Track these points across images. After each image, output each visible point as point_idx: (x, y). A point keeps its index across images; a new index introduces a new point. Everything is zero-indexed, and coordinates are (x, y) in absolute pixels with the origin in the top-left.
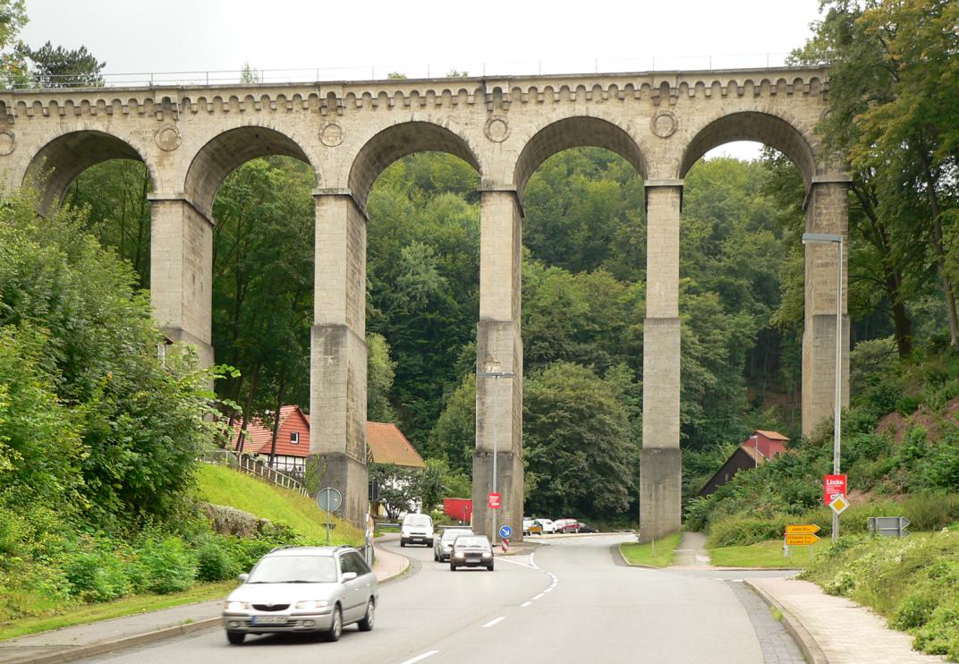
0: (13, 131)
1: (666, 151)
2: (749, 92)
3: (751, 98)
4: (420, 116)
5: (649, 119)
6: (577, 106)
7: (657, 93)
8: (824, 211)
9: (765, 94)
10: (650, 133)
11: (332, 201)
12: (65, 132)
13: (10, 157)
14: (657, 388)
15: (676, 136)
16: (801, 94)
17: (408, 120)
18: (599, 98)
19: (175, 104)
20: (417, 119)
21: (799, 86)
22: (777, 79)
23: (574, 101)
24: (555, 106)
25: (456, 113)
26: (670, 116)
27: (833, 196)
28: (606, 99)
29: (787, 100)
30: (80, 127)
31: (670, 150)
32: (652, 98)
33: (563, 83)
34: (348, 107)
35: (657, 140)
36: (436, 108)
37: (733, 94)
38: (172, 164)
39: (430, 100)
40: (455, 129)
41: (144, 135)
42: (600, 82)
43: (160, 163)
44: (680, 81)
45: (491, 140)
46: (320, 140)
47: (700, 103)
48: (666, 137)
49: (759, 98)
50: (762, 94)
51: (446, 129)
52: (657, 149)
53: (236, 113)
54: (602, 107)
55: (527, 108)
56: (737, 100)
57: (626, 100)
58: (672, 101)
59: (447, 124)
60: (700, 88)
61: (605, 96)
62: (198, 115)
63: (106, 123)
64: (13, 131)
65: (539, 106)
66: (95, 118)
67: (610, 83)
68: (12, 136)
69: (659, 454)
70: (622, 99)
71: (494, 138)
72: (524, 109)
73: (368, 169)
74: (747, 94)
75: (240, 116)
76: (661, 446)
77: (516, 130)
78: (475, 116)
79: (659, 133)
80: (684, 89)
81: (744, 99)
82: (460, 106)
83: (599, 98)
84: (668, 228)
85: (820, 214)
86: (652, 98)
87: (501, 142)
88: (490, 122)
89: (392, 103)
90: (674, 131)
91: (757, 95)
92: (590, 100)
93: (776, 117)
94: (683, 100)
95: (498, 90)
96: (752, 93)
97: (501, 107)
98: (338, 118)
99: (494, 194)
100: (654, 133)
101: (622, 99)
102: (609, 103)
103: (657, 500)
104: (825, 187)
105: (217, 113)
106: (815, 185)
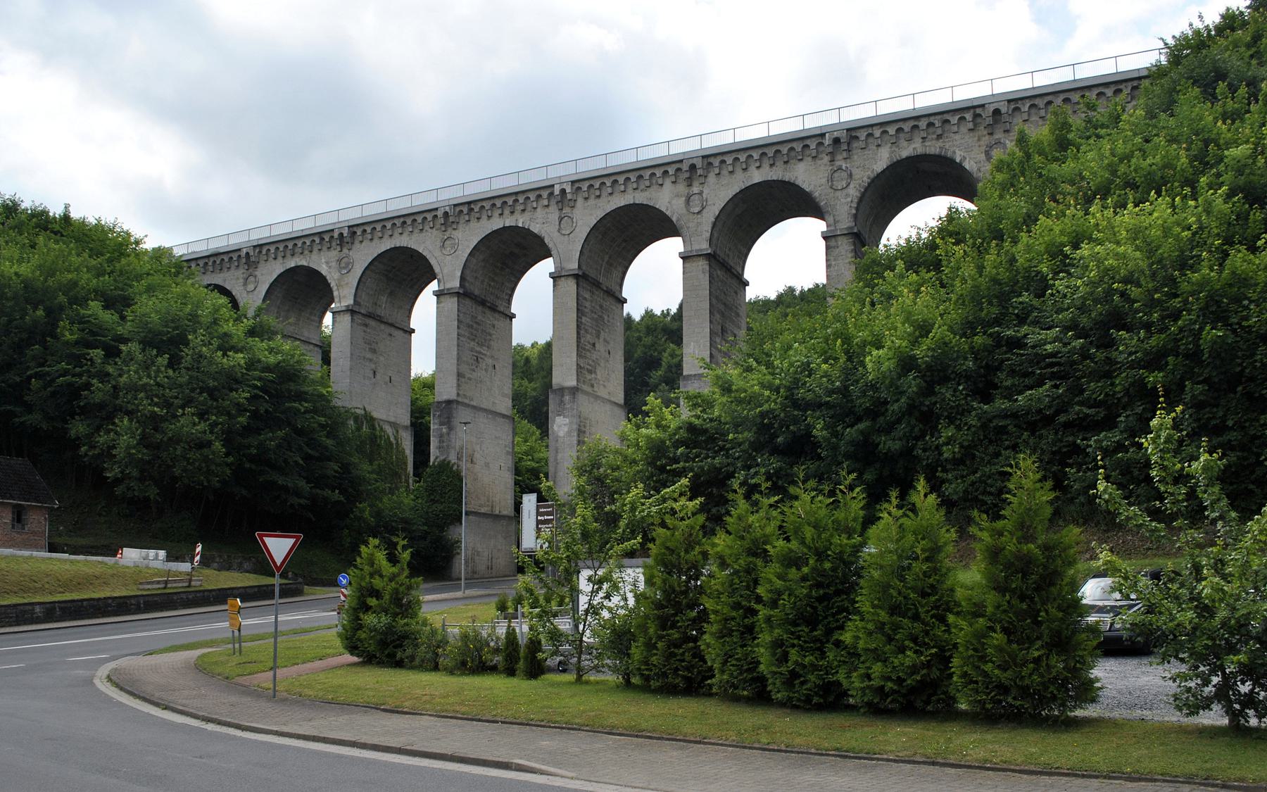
0: (256, 273)
1: (699, 224)
3: (768, 168)
4: (509, 222)
8: (833, 263)
9: (779, 163)
10: (684, 211)
13: (255, 292)
16: (810, 159)
17: (502, 226)
20: (507, 225)
21: (808, 152)
22: (787, 149)
24: (610, 198)
27: (840, 248)
30: (293, 265)
38: (347, 284)
47: (725, 179)
48: (699, 213)
49: (774, 168)
51: (529, 229)
52: (690, 225)
54: (646, 194)
55: (589, 203)
64: (256, 273)
65: (597, 200)
66: (302, 256)
71: (563, 232)
72: (586, 205)
77: (580, 223)
78: (550, 216)
88: (561, 219)
91: (771, 165)
93: (789, 183)
94: (712, 178)
98: (454, 232)
99: (563, 279)
102: (651, 189)
104: (833, 240)
105: (376, 240)
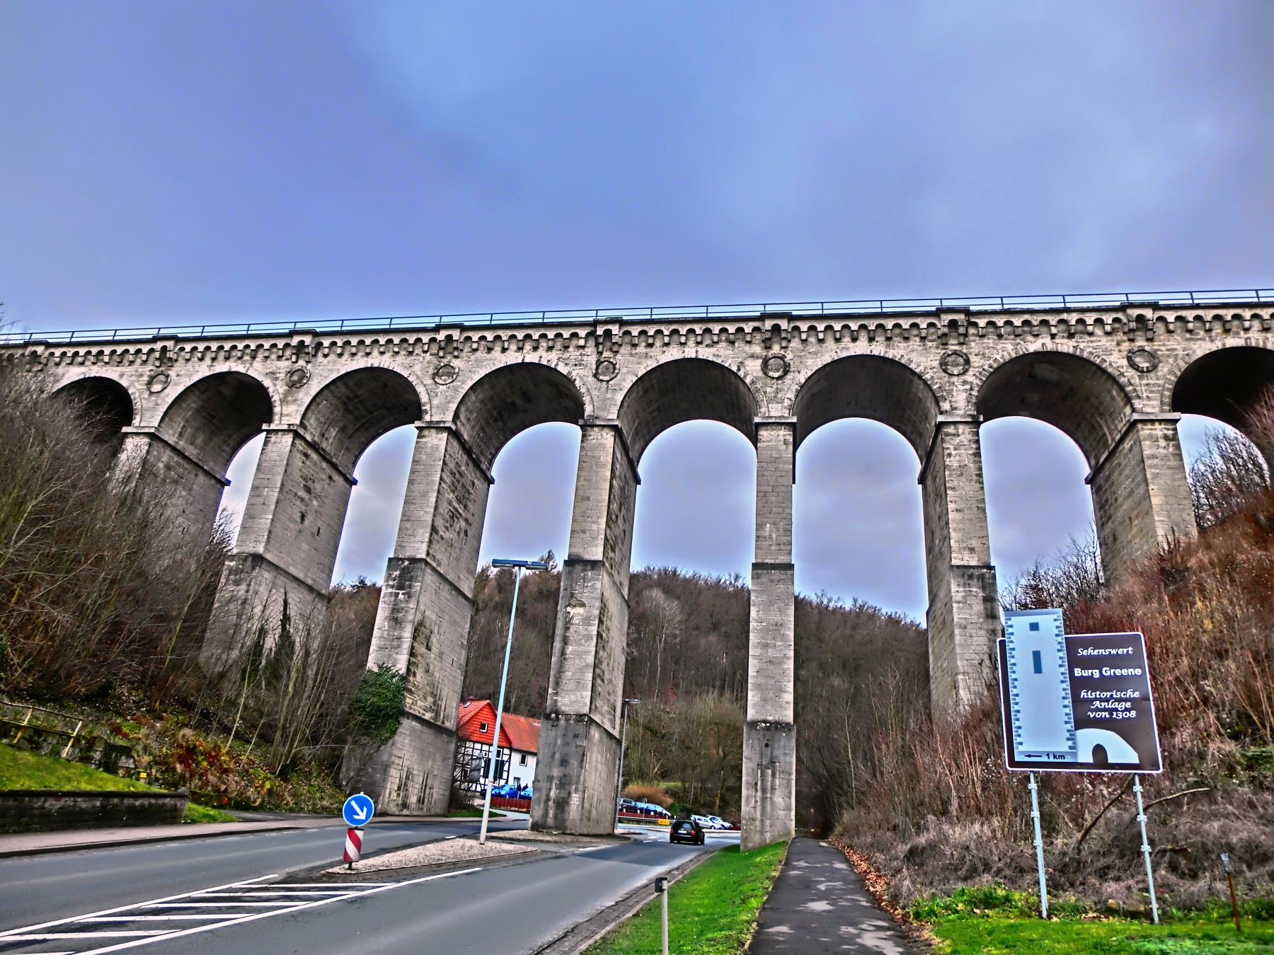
0: (170, 372)
1: (778, 391)
2: (863, 338)
3: (866, 342)
5: (761, 361)
6: (686, 349)
7: (768, 335)
8: (954, 453)
10: (761, 374)
11: (433, 431)
12: (211, 373)
13: (162, 395)
14: (766, 646)
15: (789, 376)
16: (917, 339)
17: (520, 361)
18: (709, 342)
19: (308, 346)
20: (527, 360)
23: (685, 344)
24: (665, 348)
25: (566, 355)
26: (782, 358)
28: (717, 343)
29: (903, 345)
31: (781, 390)
32: (763, 341)
33: (674, 327)
34: (466, 350)
35: (768, 381)
36: (547, 351)
37: (847, 339)
39: (544, 344)
40: (563, 369)
41: (278, 375)
42: (710, 326)
43: (283, 401)
44: (792, 325)
45: (598, 379)
46: (434, 379)
48: (778, 379)
50: (877, 339)
51: (555, 370)
52: (768, 390)
53: (362, 356)
56: (851, 345)
57: (736, 344)
58: (784, 344)
59: (557, 365)
60: (812, 333)
61: (716, 339)
62: (328, 358)
63: (248, 365)
67: (720, 327)
68: (167, 376)
69: (767, 729)
70: (732, 343)
71: (601, 378)
72: (634, 352)
73: (488, 424)
74: (861, 338)
75: (365, 359)
76: (770, 718)
78: (585, 358)
79: (771, 374)
80: (796, 333)
81: (858, 343)
82: (571, 349)
83: (709, 342)
84: (781, 466)
85: (950, 455)
86: (763, 341)
87: (608, 381)
89: (506, 345)
90: (786, 372)
92: (701, 343)
95: (608, 333)
96: (866, 338)
97: (611, 350)
99: (596, 429)
100: (766, 374)
101: (732, 343)
103: (764, 791)
106: (941, 425)
